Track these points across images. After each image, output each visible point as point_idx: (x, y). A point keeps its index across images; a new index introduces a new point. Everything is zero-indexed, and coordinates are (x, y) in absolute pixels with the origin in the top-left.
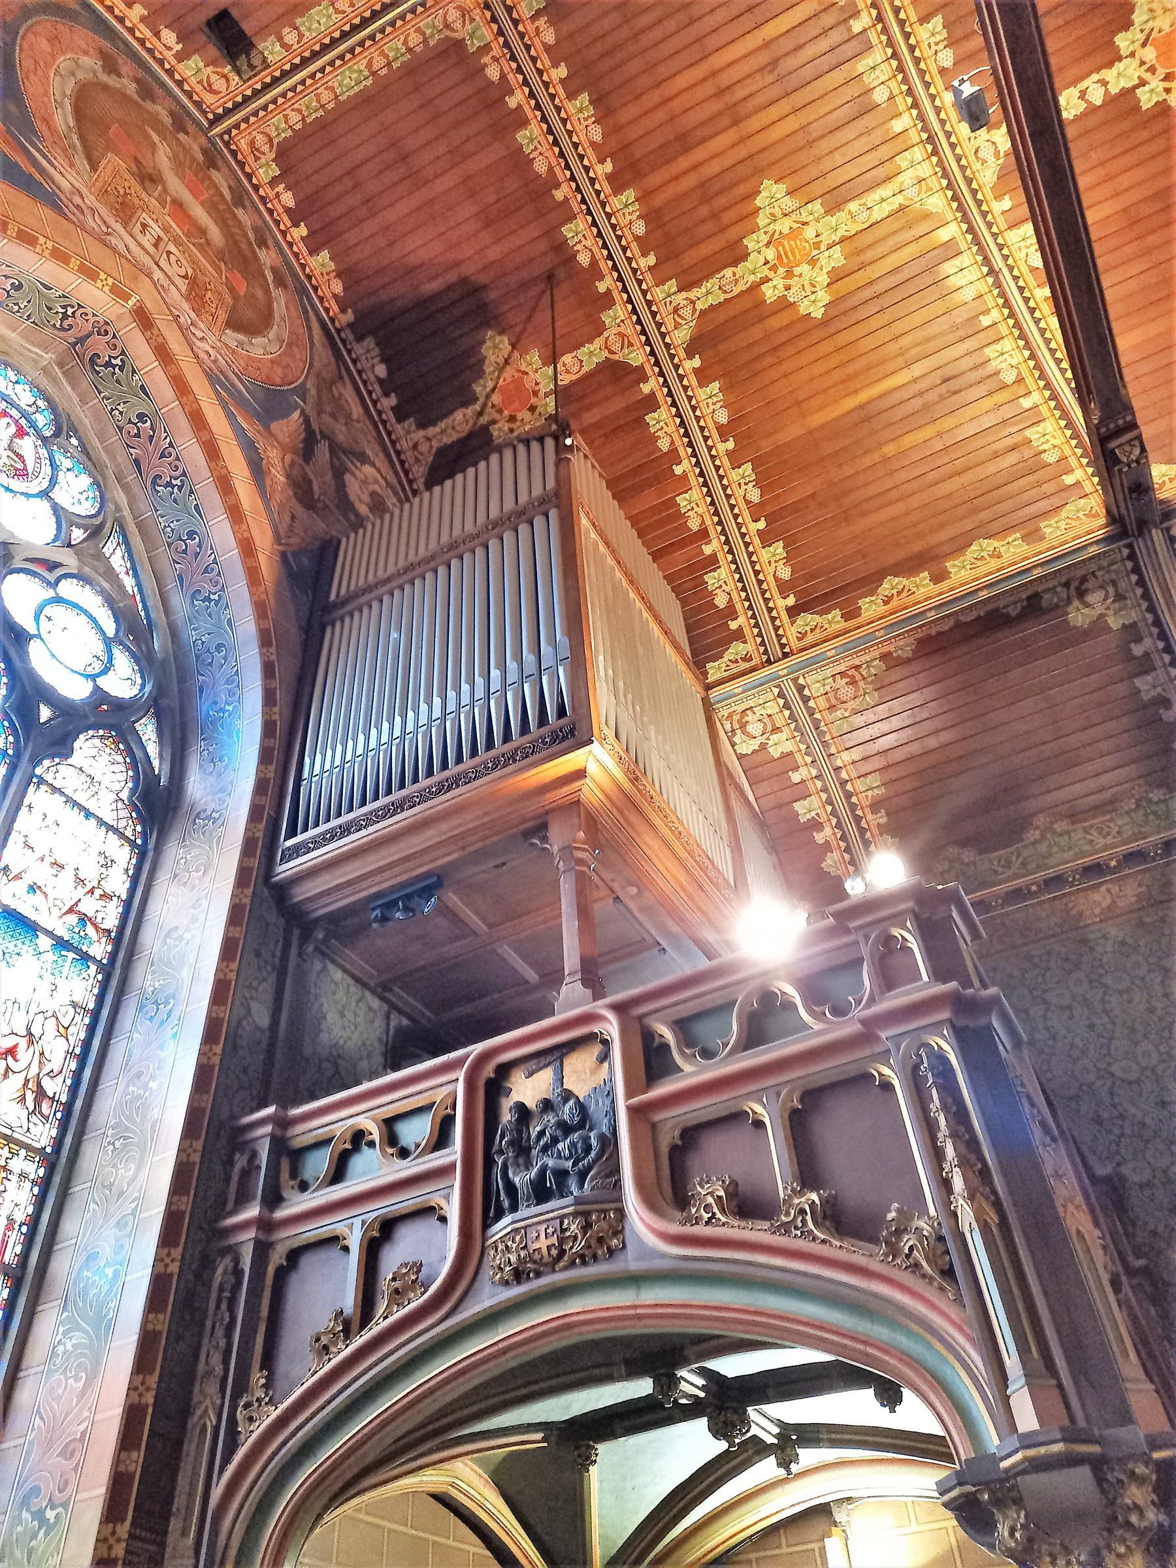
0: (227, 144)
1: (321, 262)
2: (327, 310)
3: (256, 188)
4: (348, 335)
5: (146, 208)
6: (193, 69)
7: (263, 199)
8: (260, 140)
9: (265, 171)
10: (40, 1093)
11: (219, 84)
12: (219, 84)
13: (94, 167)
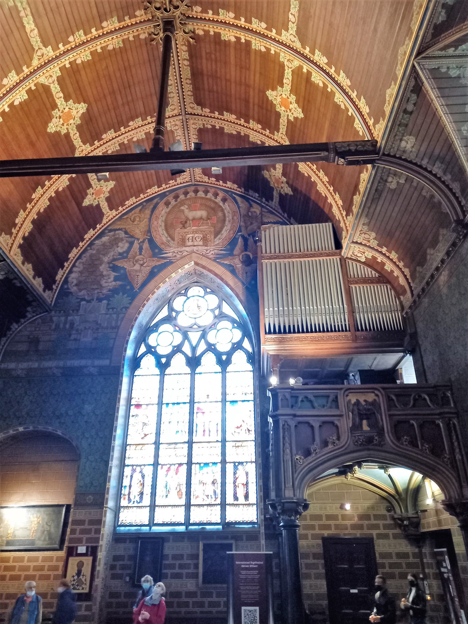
0: (197, 181)
1: (229, 184)
2: (239, 191)
3: (208, 183)
4: (246, 192)
5: (187, 233)
6: (179, 180)
7: (211, 183)
8: (199, 175)
9: (206, 179)
10: (249, 430)
11: (185, 176)
12: (185, 176)
13: (174, 240)
